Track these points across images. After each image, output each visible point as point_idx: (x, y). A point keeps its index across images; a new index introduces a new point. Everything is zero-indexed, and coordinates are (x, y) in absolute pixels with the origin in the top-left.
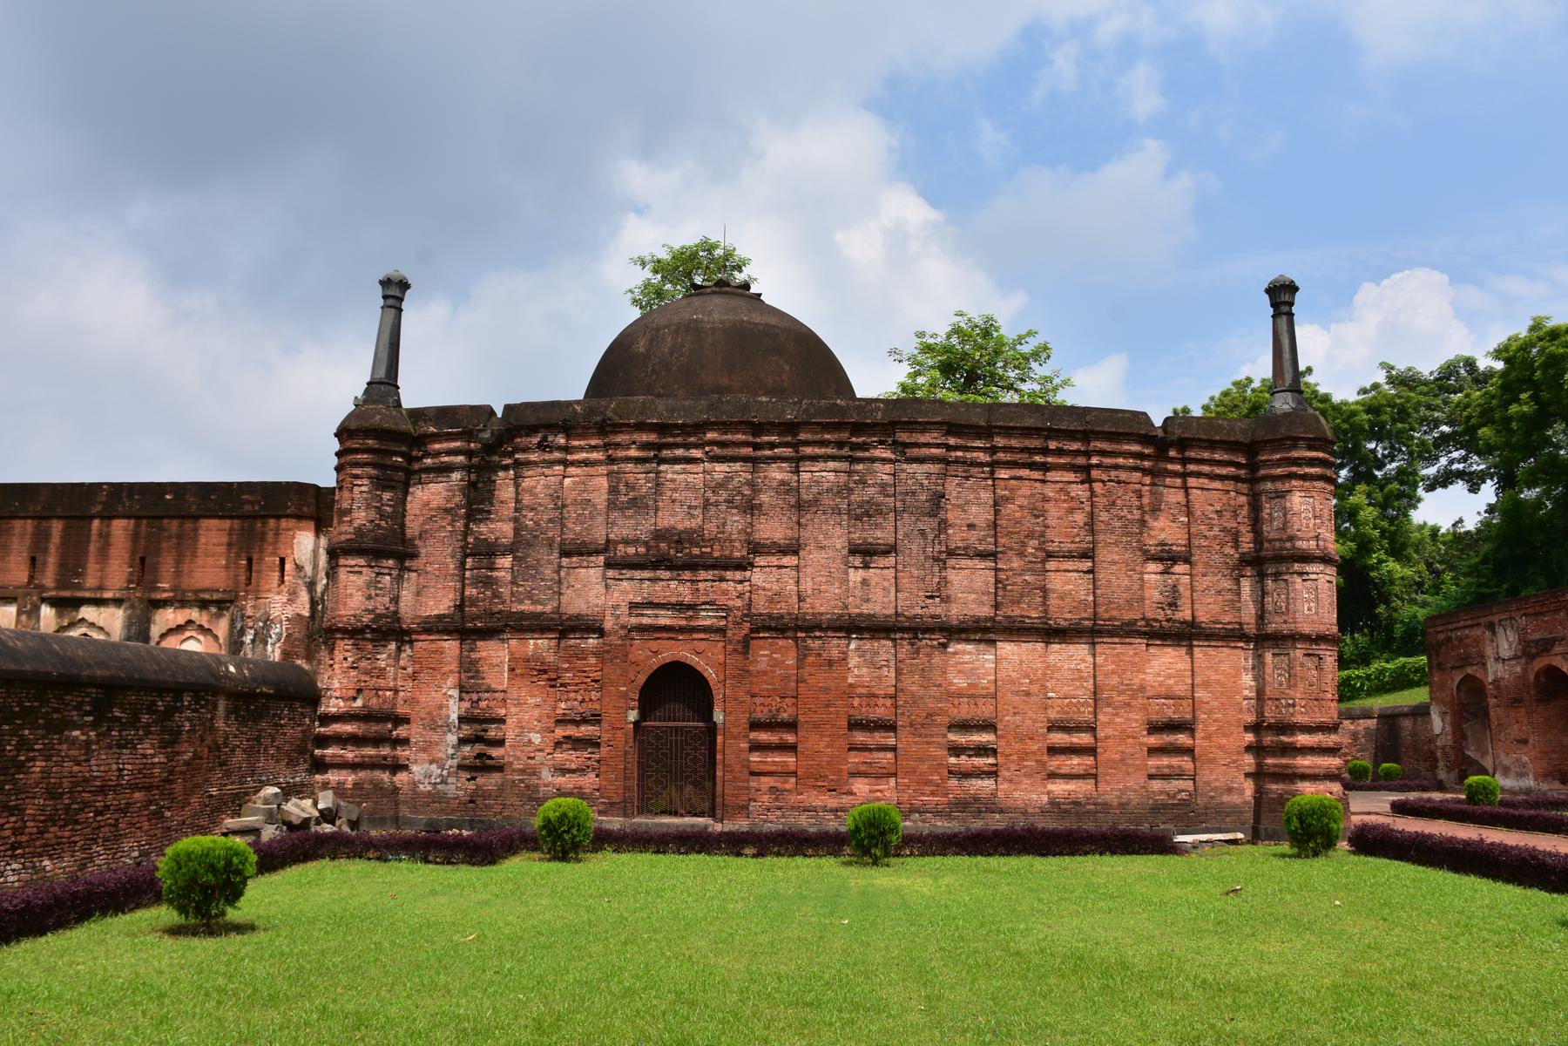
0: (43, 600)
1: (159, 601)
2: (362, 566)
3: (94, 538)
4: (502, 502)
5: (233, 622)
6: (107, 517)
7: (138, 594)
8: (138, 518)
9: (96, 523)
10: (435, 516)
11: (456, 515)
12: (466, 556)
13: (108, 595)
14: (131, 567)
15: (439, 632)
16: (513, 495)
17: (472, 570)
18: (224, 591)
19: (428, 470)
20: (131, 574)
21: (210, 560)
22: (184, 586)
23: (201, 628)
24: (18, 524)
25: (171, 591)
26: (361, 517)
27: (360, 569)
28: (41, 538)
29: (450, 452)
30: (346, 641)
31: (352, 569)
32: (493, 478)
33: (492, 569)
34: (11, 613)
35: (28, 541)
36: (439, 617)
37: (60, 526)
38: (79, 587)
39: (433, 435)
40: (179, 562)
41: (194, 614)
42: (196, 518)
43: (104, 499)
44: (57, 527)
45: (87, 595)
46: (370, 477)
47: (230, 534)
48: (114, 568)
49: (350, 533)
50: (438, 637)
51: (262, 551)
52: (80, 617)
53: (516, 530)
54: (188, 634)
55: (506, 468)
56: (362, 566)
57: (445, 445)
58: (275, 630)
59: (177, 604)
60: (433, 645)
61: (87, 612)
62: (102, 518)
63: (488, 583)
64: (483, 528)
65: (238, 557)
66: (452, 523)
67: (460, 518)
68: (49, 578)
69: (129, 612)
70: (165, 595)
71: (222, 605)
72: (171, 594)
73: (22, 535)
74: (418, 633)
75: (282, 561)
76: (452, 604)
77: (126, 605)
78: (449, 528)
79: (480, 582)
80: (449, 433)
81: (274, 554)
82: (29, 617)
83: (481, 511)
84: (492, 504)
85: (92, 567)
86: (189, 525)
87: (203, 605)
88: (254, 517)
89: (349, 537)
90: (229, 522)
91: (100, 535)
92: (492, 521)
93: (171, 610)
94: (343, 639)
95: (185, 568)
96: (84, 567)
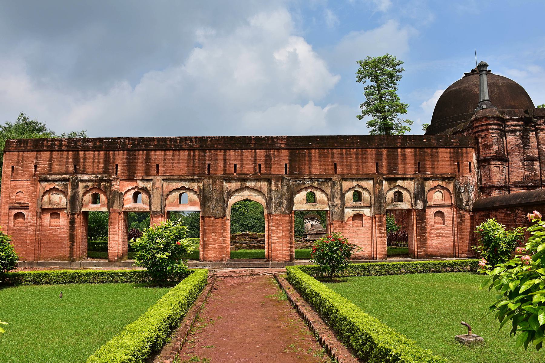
0: (384, 178)
1: (427, 178)
2: (499, 165)
3: (399, 156)
4: (532, 142)
5: (455, 185)
6: (403, 148)
7: (420, 176)
8: (415, 148)
9: (399, 150)
10: (513, 147)
11: (520, 147)
12: (525, 161)
13: (409, 176)
14: (415, 166)
15: (520, 187)
16: (536, 140)
17: (526, 166)
18: (451, 174)
19: (508, 131)
20: (415, 168)
21: (444, 163)
22: (436, 173)
23: (443, 188)
24: (369, 150)
25: (431, 174)
26: (495, 148)
27: (499, 166)
28: (379, 157)
29: (514, 125)
30: (496, 191)
31: (496, 166)
32: (529, 134)
33: (533, 165)
34: (370, 183)
35: (374, 157)
36: (519, 182)
37: (386, 151)
38: (396, 174)
39: (509, 119)
40: (433, 164)
41: (440, 183)
42: (437, 148)
43: (400, 141)
44: (384, 151)
45: (401, 176)
46: (498, 134)
47: (450, 154)
48: (409, 166)
49: (494, 153)
50: (519, 189)
51: (462, 160)
52: (397, 184)
53: (539, 152)
54: (437, 190)
55: (532, 131)
56: (499, 165)
57: (512, 123)
58: (471, 188)
59: (433, 179)
60: (518, 192)
61: (400, 183)
62: (401, 148)
63: (532, 170)
64: (528, 151)
65: (454, 162)
66: (519, 149)
67: (522, 148)
68: (384, 170)
69: (417, 182)
70: (430, 176)
71: (450, 179)
72: (432, 176)
73: (372, 155)
74: (512, 187)
75: (470, 163)
76: (522, 177)
77: (416, 180)
78: (518, 151)
79: (530, 170)
80: (514, 119)
81: (467, 161)
82: (379, 185)
83: (526, 146)
84: (529, 143)
85: (400, 166)
86: (434, 150)
87: (443, 179)
88: (458, 148)
89: (494, 154)
90: (449, 149)
91: (402, 155)
92: (530, 149)
93: (431, 181)
94: (495, 190)
95: (435, 166)
96: (397, 166)
